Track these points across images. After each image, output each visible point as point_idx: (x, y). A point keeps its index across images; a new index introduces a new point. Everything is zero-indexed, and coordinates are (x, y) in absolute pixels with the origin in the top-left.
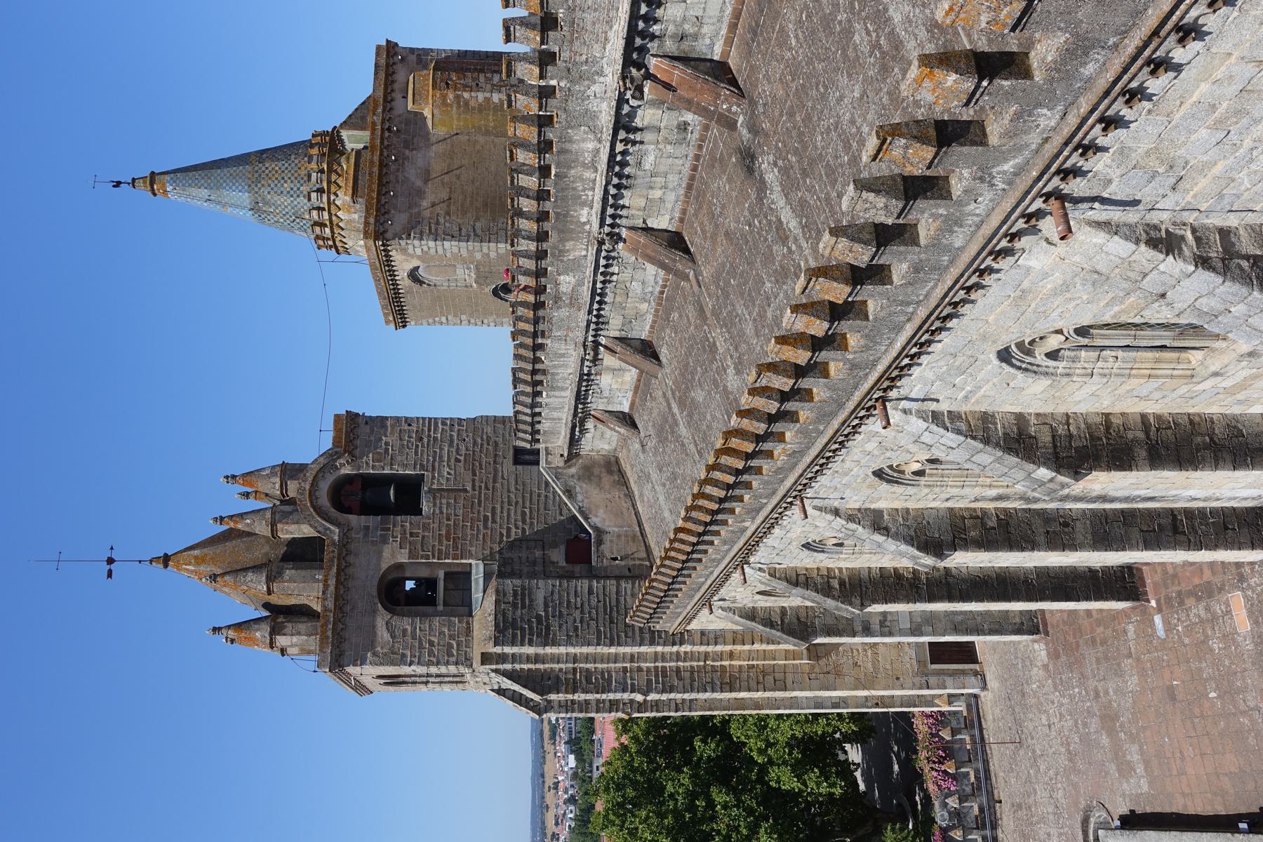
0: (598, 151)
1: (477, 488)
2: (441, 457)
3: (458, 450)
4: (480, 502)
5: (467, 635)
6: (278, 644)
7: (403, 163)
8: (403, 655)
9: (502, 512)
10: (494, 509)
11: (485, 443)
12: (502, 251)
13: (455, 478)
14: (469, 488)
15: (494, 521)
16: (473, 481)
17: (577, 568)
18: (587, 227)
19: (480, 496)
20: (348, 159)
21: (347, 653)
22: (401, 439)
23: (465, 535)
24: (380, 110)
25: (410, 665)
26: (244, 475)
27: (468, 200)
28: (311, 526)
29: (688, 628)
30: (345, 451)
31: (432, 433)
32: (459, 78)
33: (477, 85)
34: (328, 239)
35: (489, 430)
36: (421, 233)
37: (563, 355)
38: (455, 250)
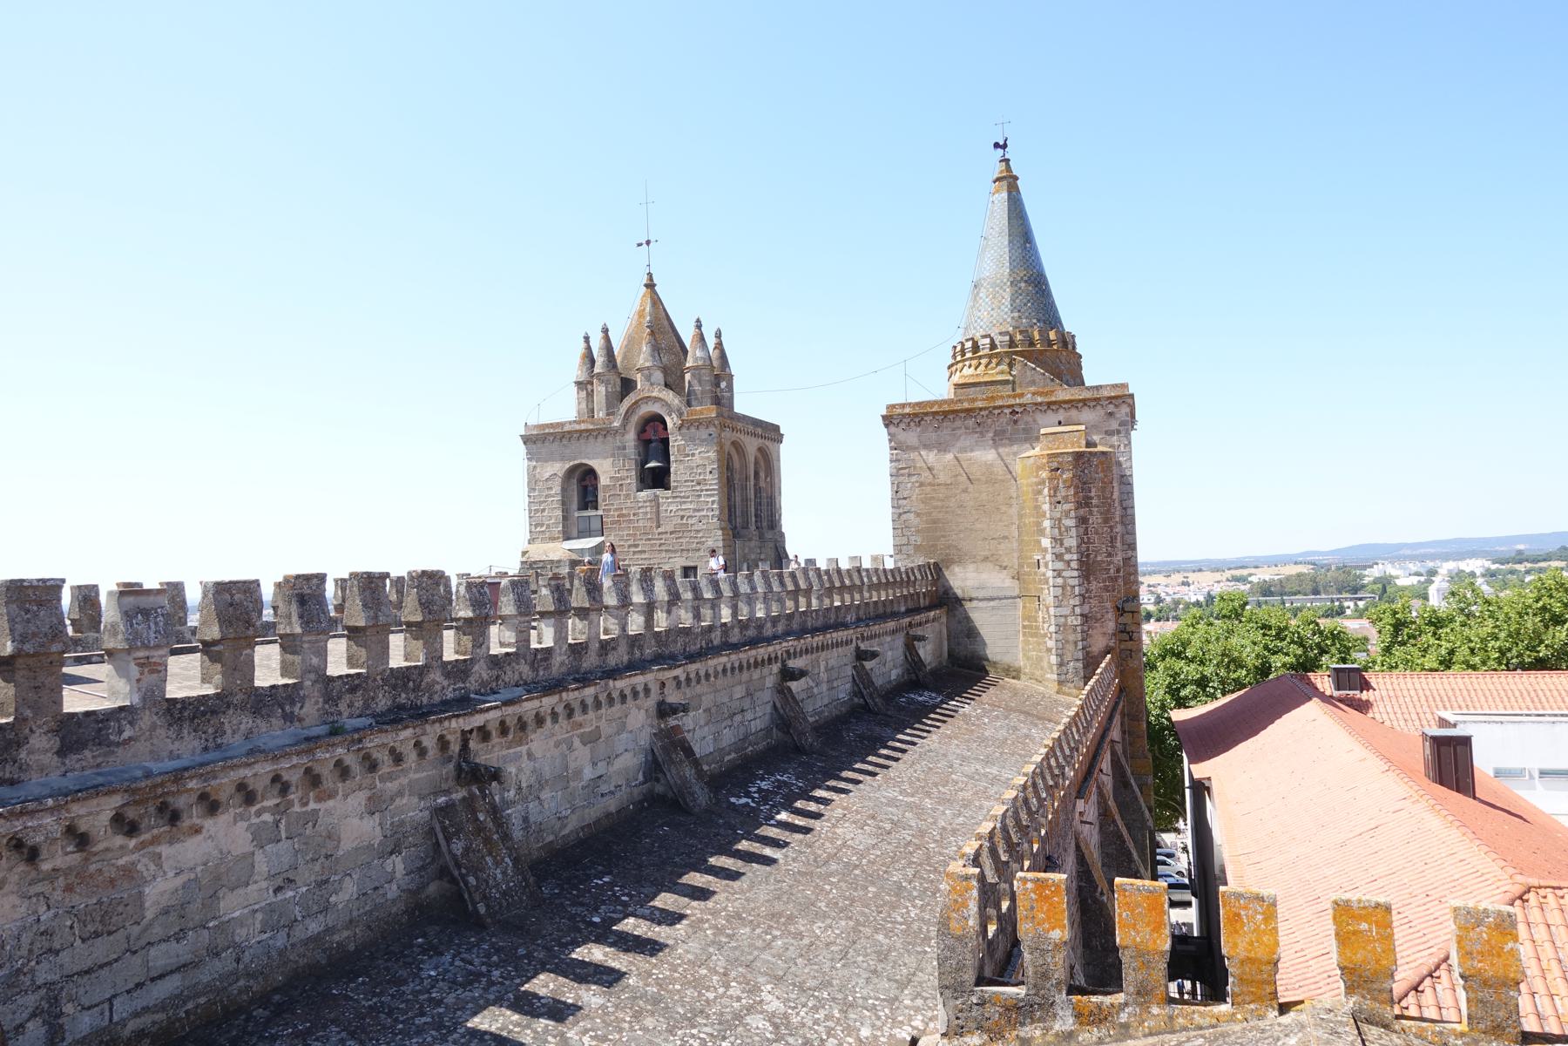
2: (685, 502)
3: (691, 517)
4: (649, 540)
7: (977, 432)
8: (534, 489)
10: (645, 552)
14: (660, 530)
15: (634, 553)
20: (1002, 372)
24: (1039, 399)
26: (702, 335)
27: (939, 504)
30: (683, 420)
32: (1064, 482)
33: (1059, 502)
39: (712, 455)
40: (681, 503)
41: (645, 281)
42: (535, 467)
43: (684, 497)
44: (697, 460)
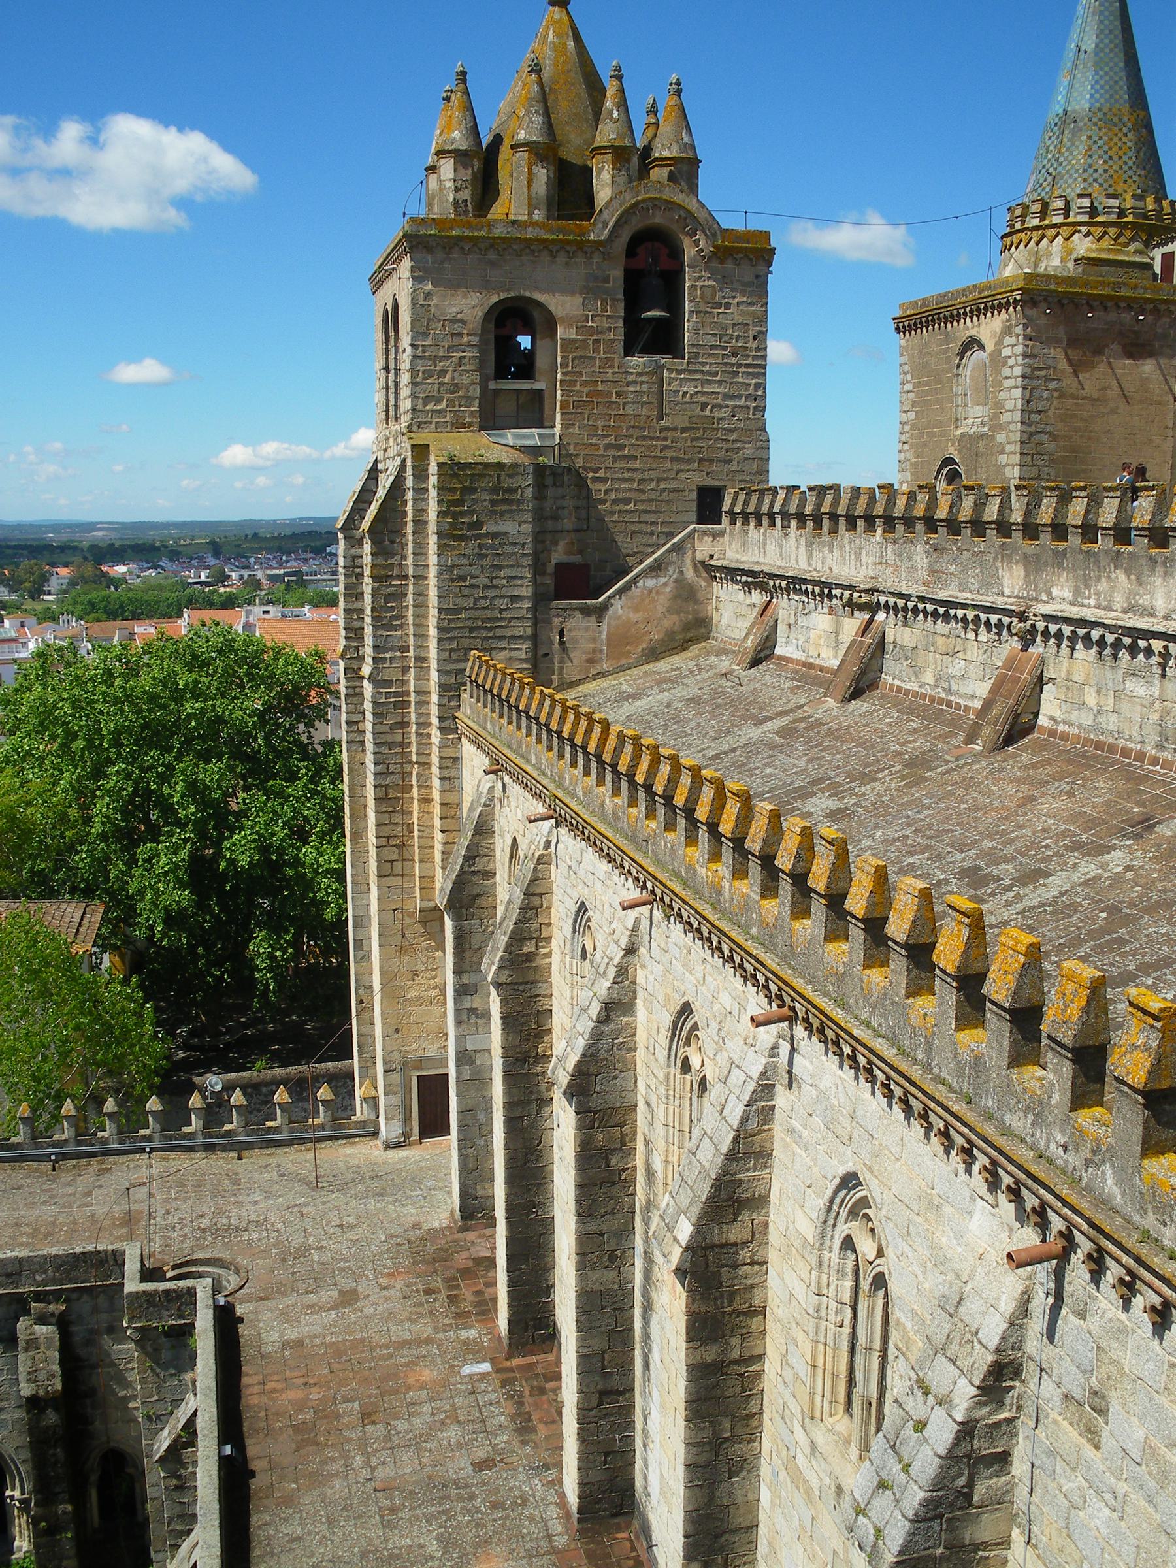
0: (1152, 615)
1: (663, 434)
2: (709, 382)
3: (720, 406)
4: (644, 438)
5: (453, 424)
6: (443, 161)
8: (426, 335)
9: (629, 470)
10: (635, 458)
11: (730, 445)
12: (1008, 472)
13: (679, 403)
15: (615, 459)
16: (675, 429)
17: (549, 581)
18: (1044, 598)
19: (652, 438)
20: (1137, 252)
21: (429, 257)
22: (734, 325)
25: (412, 345)
28: (611, 200)
29: (463, 739)
34: (1023, 222)
35: (748, 452)
36: (1033, 356)
37: (858, 558)
38: (1009, 405)
40: (704, 382)
42: (428, 295)
43: (707, 373)
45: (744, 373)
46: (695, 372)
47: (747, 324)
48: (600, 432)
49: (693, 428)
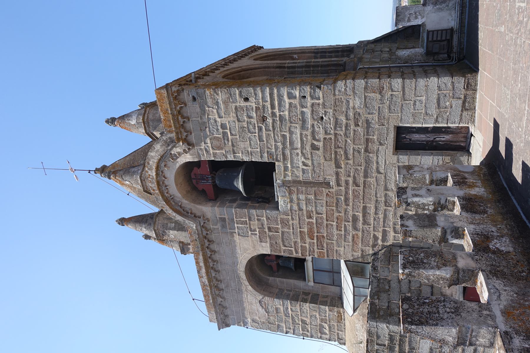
2: (292, 143)
3: (313, 133)
4: (346, 200)
8: (279, 326)
9: (376, 214)
10: (365, 208)
11: (352, 123)
13: (313, 170)
14: (333, 183)
16: (337, 174)
19: (347, 193)
22: (239, 121)
23: (330, 237)
25: (286, 333)
26: (119, 118)
30: (179, 140)
31: (276, 110)
39: (221, 96)
40: (293, 148)
41: (98, 175)
43: (284, 144)
44: (229, 120)
45: (279, 110)
46: (284, 154)
47: (236, 108)
48: (343, 233)
49: (336, 157)
